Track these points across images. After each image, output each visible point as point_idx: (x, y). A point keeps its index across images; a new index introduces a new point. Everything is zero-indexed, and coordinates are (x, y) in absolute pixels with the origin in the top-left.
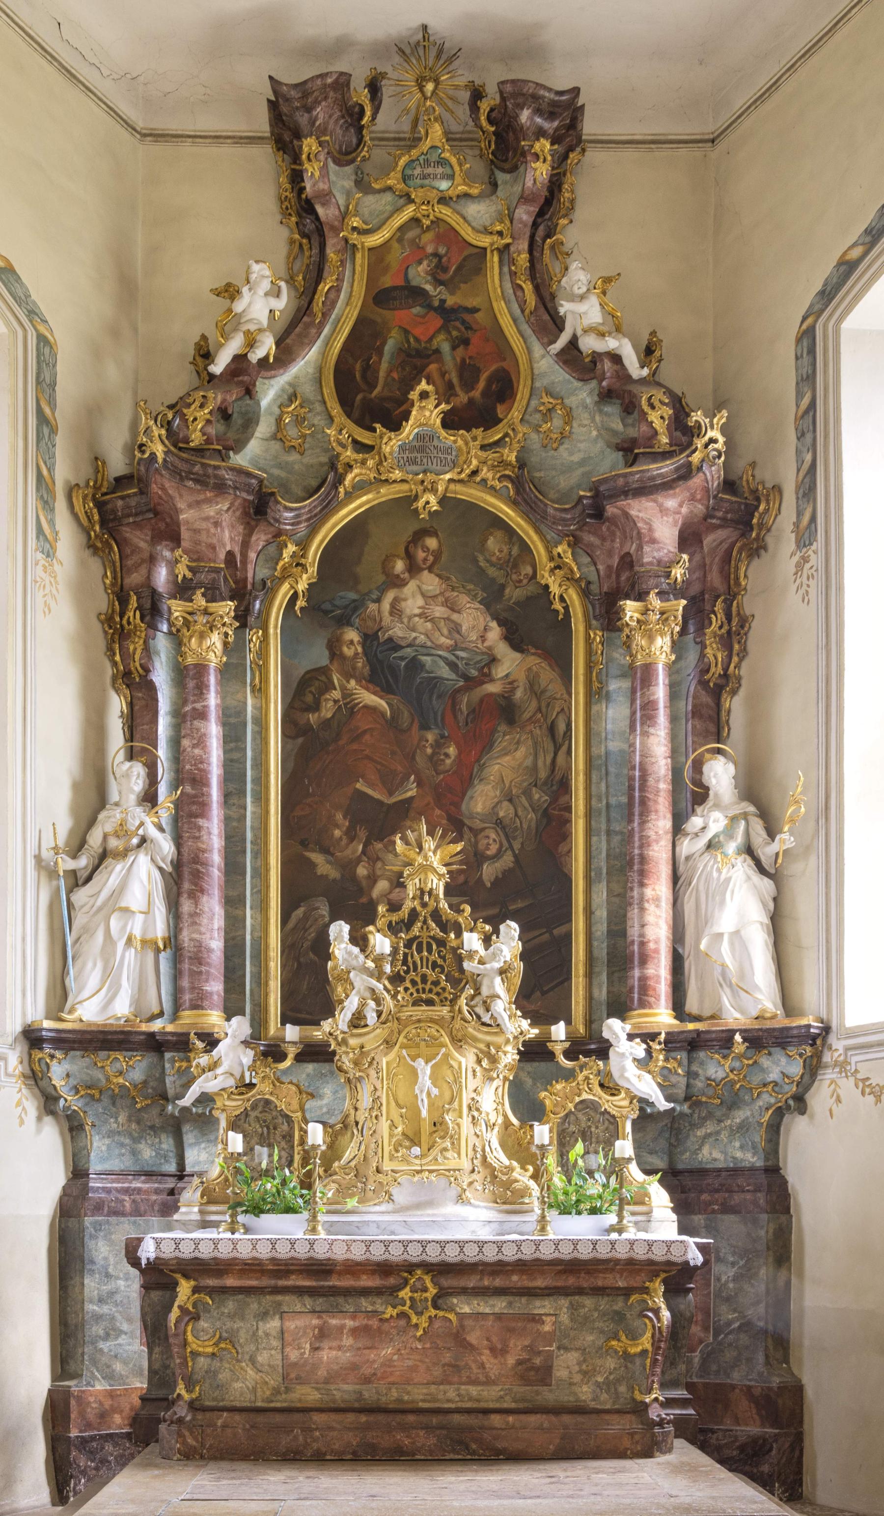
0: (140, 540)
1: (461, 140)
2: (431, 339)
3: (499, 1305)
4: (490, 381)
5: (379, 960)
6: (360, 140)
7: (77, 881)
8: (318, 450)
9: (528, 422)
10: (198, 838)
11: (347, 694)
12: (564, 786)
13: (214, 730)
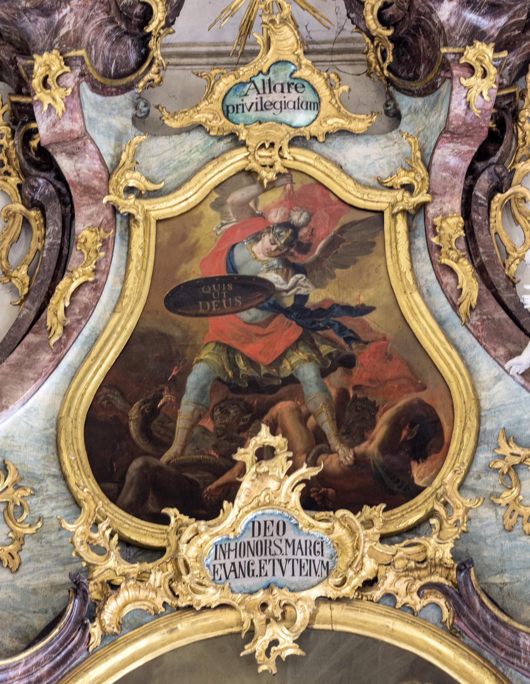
1: (332, 52)
2: (278, 361)
4: (396, 425)
6: (144, 56)
8: (49, 562)
9: (474, 490)
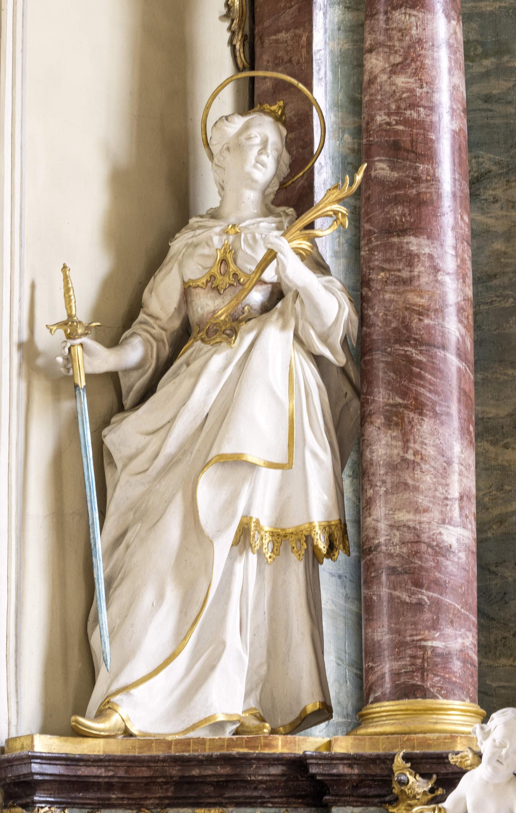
7: (117, 396)
10: (408, 282)
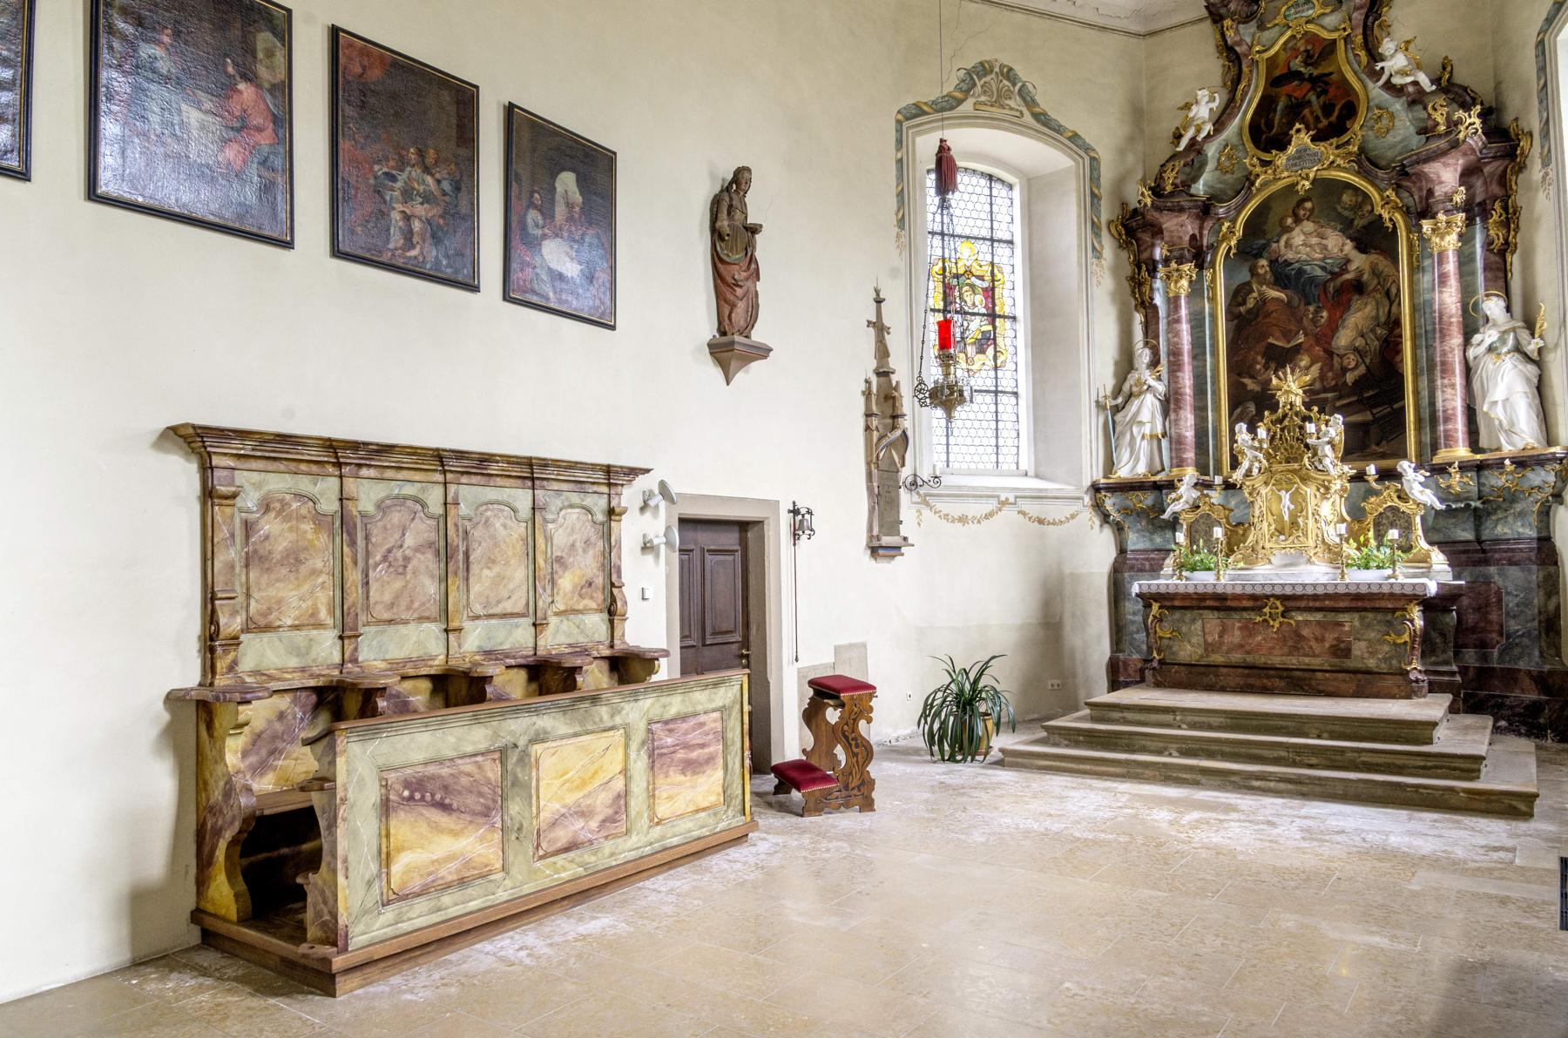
0: (1146, 237)
3: (1319, 616)
5: (1260, 442)
7: (1117, 409)
11: (1261, 294)
12: (1397, 323)
13: (1185, 328)
